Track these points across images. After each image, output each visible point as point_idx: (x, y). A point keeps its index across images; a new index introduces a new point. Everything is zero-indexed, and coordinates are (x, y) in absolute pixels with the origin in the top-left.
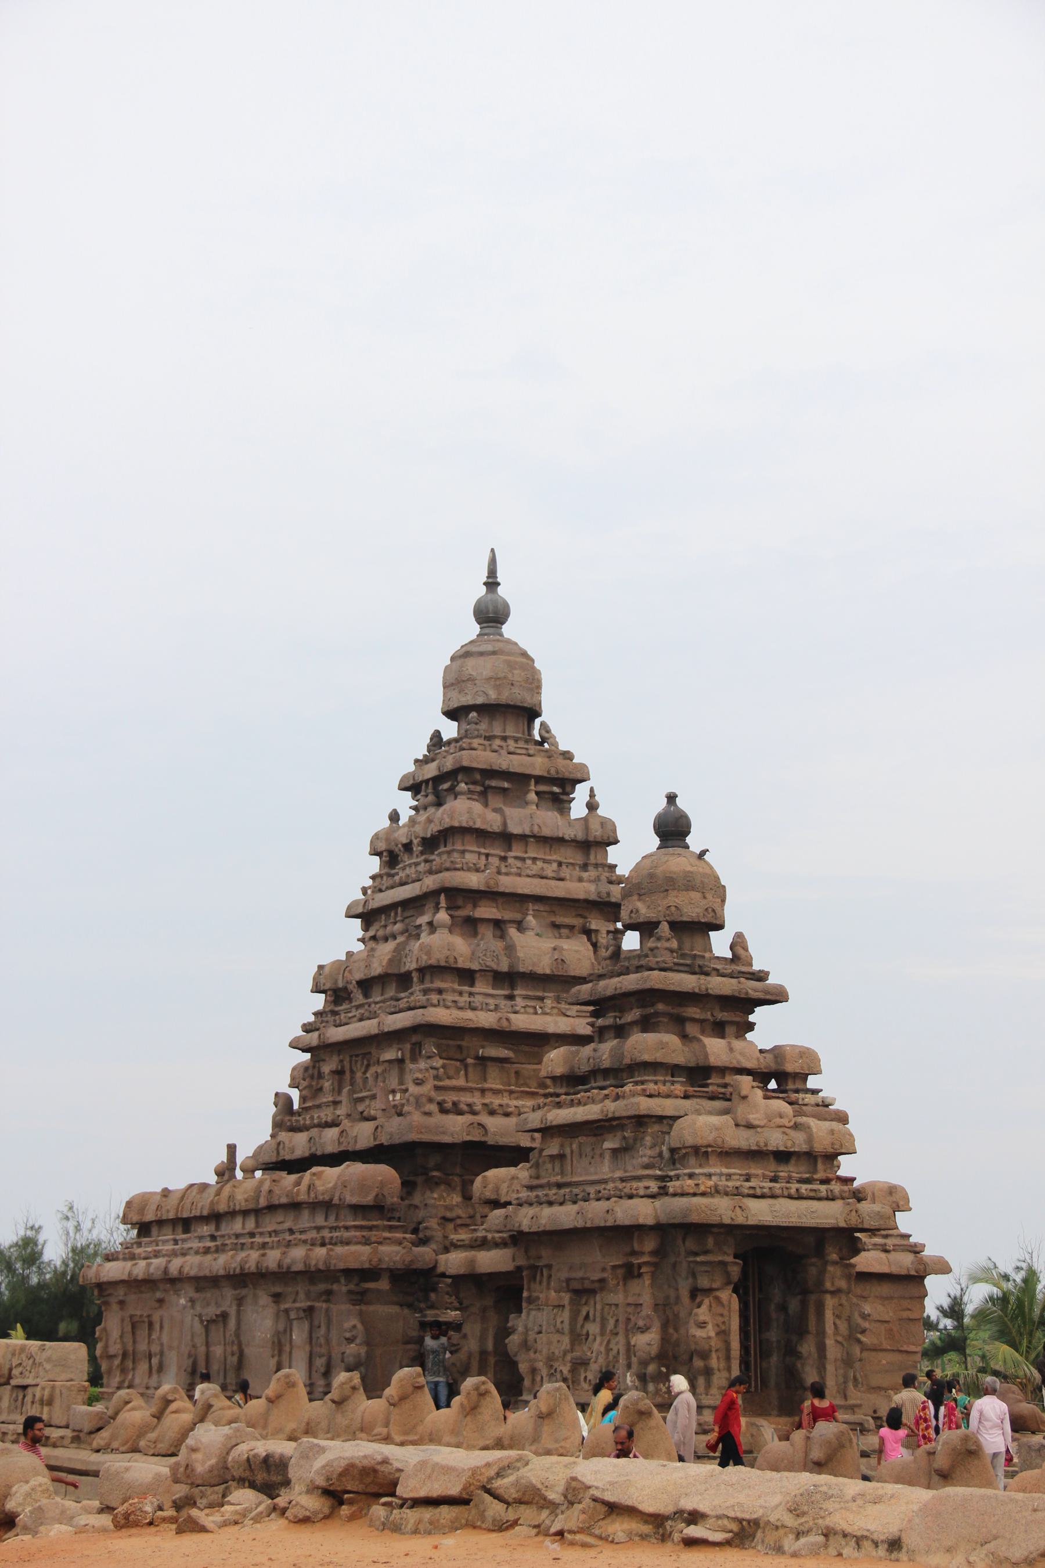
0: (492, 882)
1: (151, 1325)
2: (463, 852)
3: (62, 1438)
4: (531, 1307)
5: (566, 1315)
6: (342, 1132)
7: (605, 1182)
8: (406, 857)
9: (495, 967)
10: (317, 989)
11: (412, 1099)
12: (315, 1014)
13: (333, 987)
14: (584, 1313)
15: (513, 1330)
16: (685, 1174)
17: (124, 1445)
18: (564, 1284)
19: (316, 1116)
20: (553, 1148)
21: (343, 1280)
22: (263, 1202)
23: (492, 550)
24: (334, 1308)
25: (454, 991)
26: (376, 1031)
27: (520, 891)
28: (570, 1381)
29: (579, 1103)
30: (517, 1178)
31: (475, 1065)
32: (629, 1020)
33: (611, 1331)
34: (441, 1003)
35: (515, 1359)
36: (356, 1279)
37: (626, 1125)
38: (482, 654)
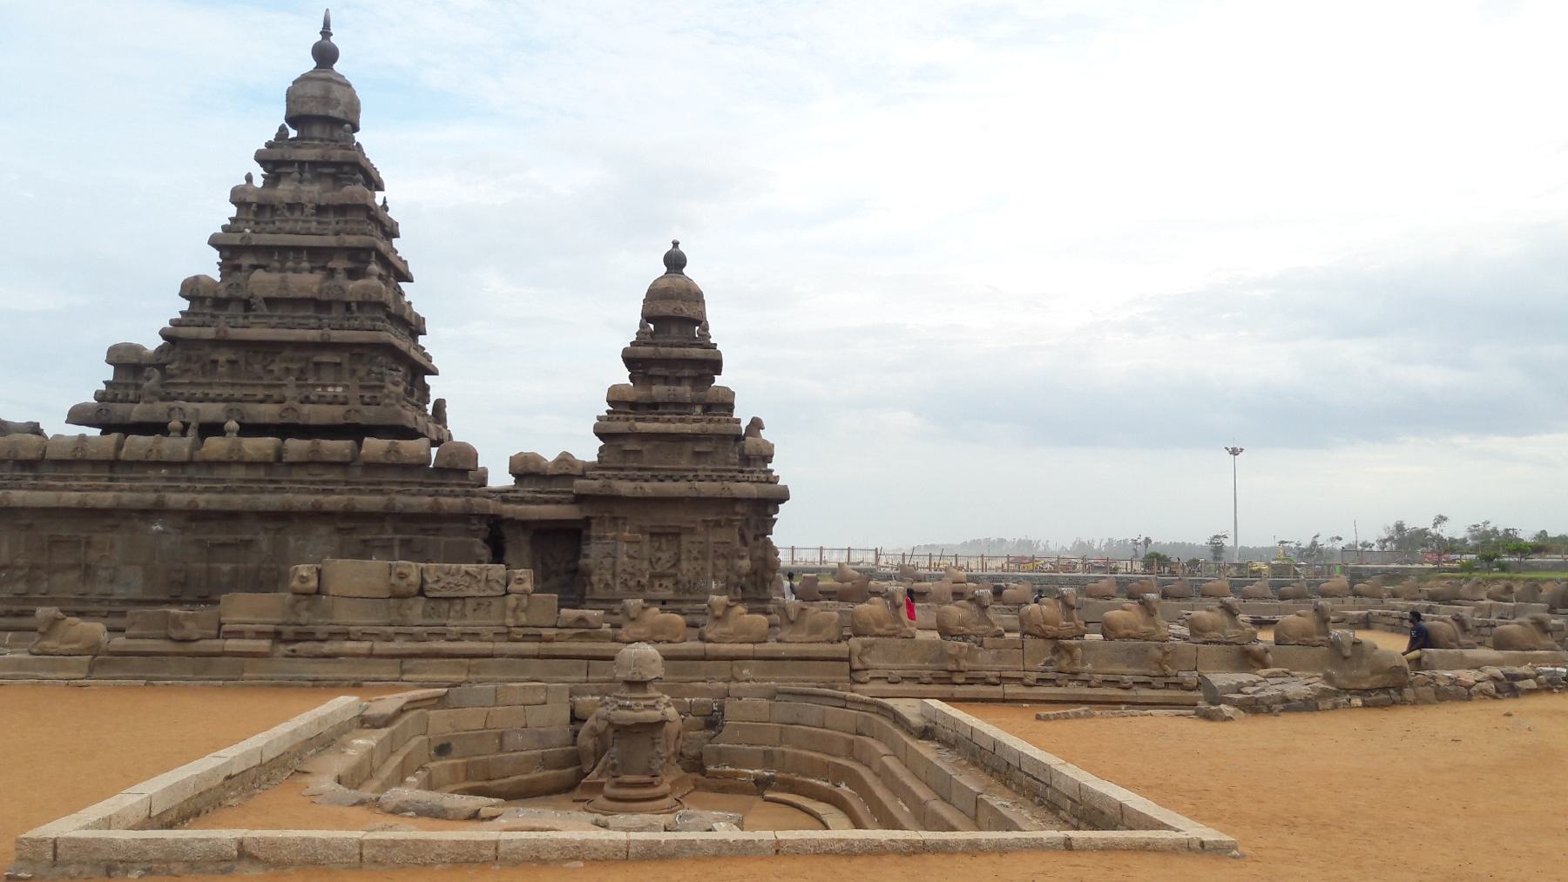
1: (88, 544)
3: (557, 635)
5: (646, 549)
6: (287, 409)
7: (696, 470)
8: (288, 214)
11: (393, 395)
12: (181, 312)
14: (657, 545)
15: (586, 556)
16: (761, 471)
17: (678, 636)
19: (212, 393)
20: (631, 446)
21: (475, 521)
22: (288, 458)
23: (327, 10)
24: (443, 540)
26: (318, 340)
29: (669, 420)
30: (567, 460)
32: (686, 374)
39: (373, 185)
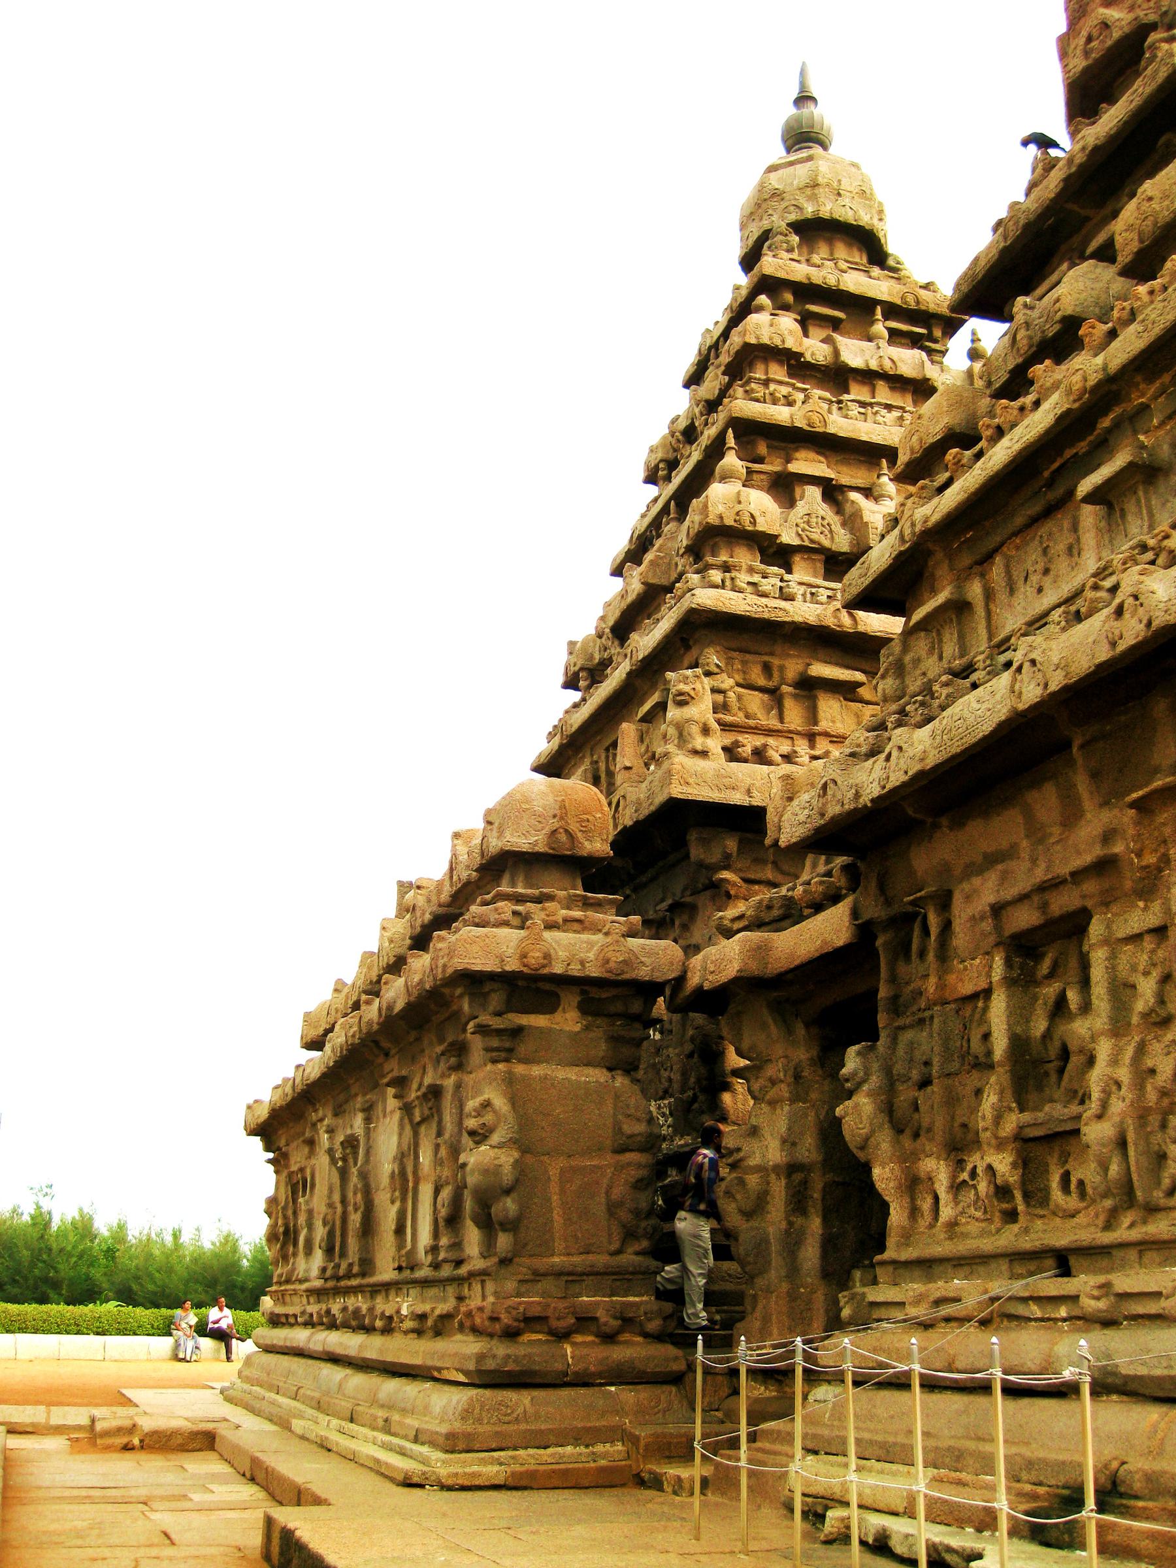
0: (816, 418)
2: (766, 383)
4: (900, 1022)
9: (826, 543)
10: (571, 683)
13: (589, 664)
18: (987, 925)
23: (804, 64)
25: (751, 570)
27: (865, 438)
28: (1018, 1195)
31: (795, 697)
33: (1145, 1016)
34: (728, 583)
35: (861, 1156)
36: (496, 1000)
37: (1145, 408)
38: (791, 164)
39: (879, 310)
